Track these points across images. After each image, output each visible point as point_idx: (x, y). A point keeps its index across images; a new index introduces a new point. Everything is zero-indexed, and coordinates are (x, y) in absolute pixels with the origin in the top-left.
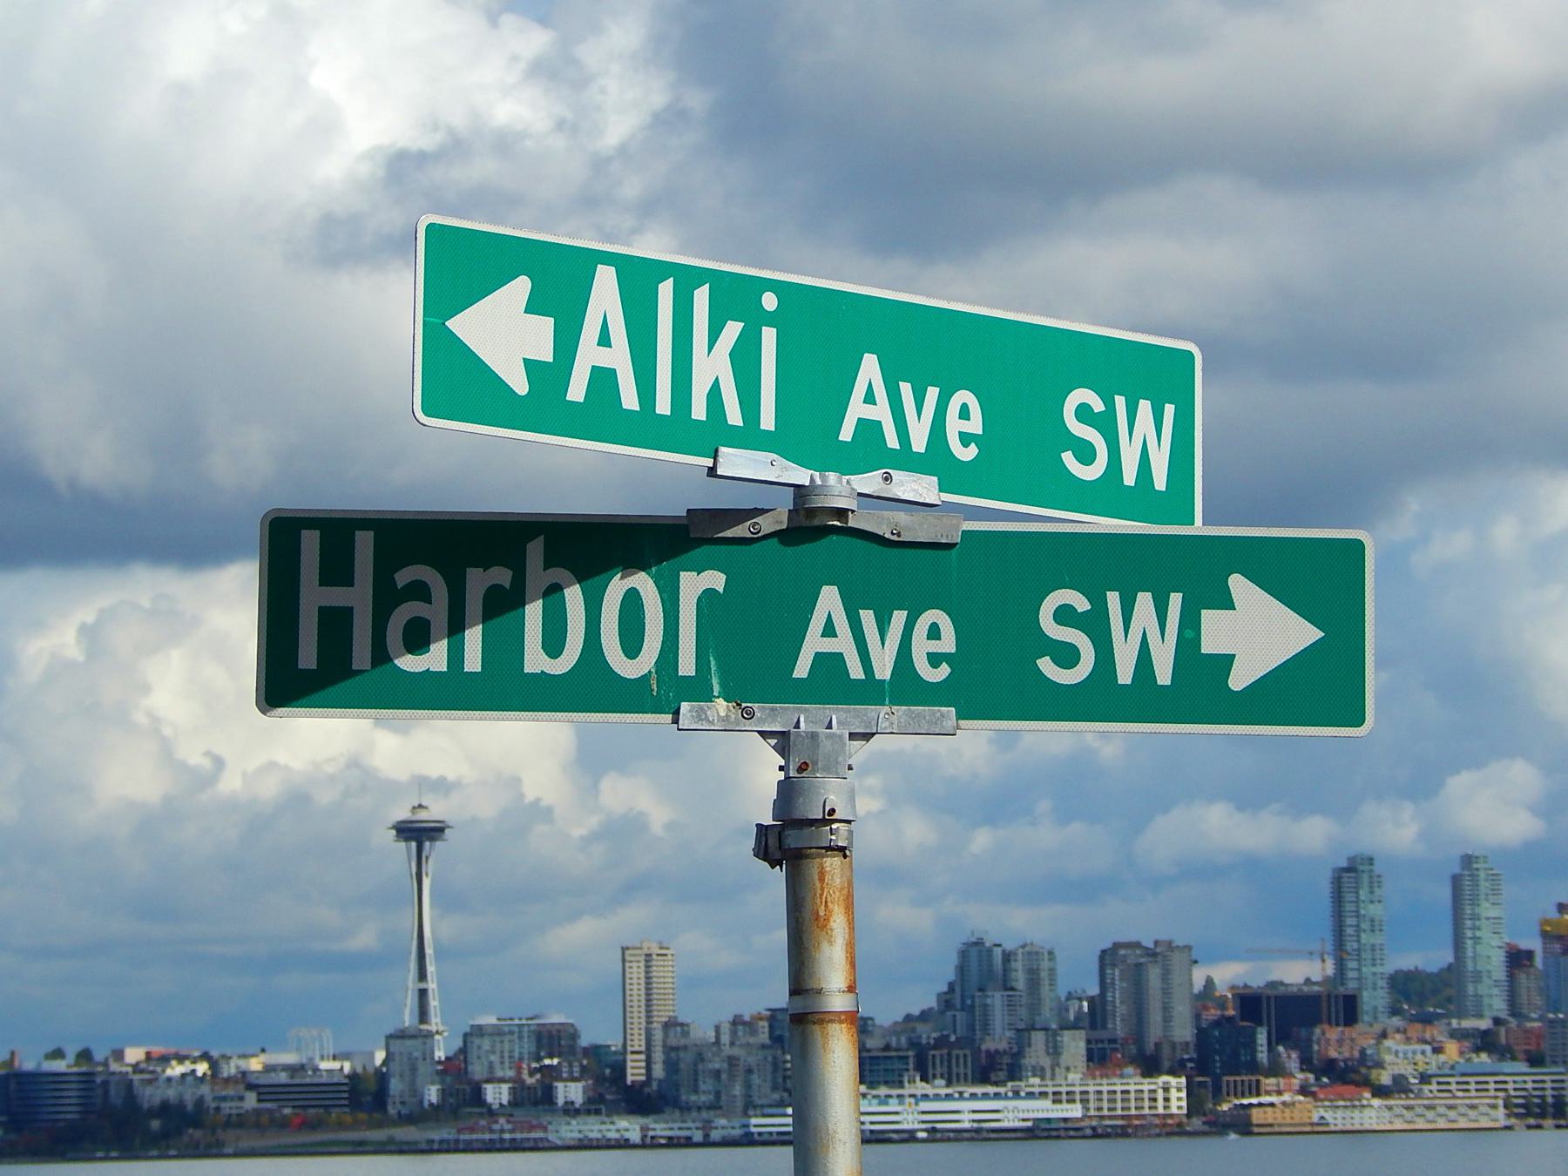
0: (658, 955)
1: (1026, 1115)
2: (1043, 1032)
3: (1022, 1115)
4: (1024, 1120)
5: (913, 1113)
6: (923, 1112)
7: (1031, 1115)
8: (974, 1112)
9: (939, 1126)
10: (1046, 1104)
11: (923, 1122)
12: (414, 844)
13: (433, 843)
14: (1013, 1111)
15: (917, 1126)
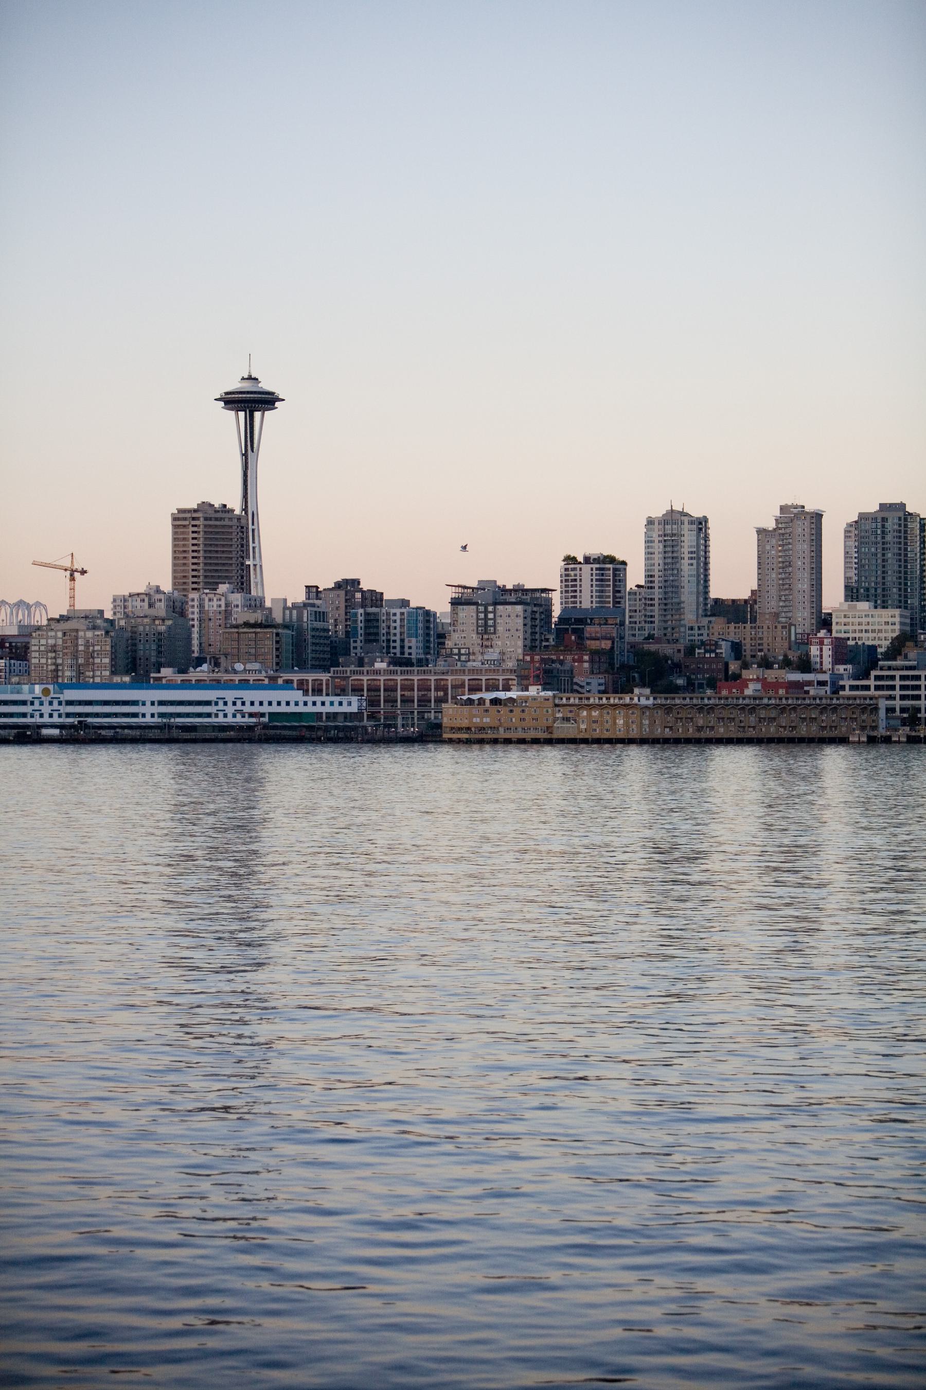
0: (206, 519)
1: (256, 709)
2: (474, 607)
3: (248, 709)
4: (251, 715)
5: (51, 703)
6: (70, 703)
7: (266, 709)
8: (161, 703)
9: (89, 720)
10: (297, 695)
11: (68, 715)
12: (242, 414)
13: (266, 413)
14: (234, 704)
15: (56, 719)
